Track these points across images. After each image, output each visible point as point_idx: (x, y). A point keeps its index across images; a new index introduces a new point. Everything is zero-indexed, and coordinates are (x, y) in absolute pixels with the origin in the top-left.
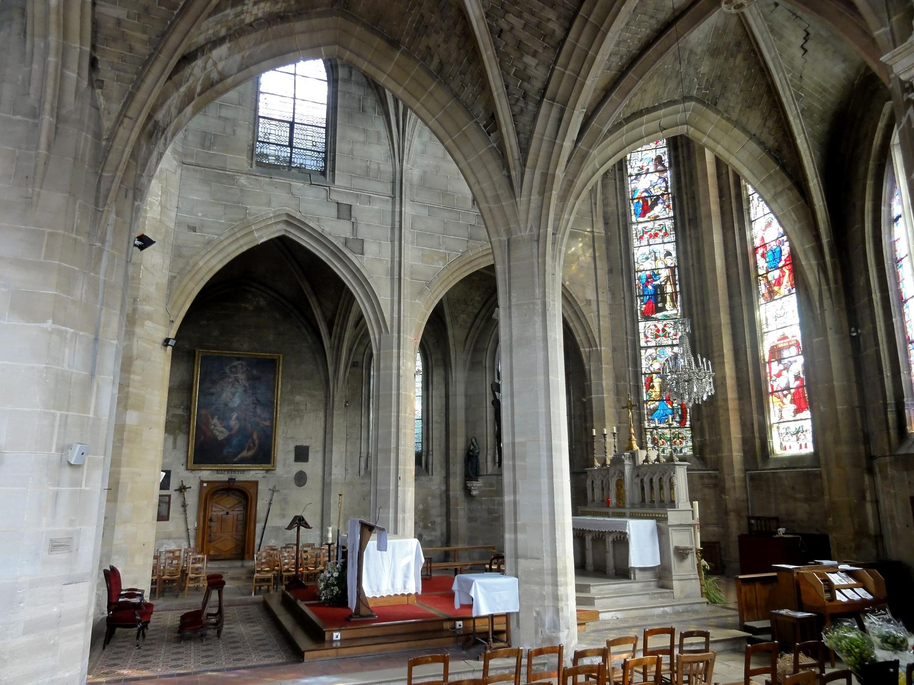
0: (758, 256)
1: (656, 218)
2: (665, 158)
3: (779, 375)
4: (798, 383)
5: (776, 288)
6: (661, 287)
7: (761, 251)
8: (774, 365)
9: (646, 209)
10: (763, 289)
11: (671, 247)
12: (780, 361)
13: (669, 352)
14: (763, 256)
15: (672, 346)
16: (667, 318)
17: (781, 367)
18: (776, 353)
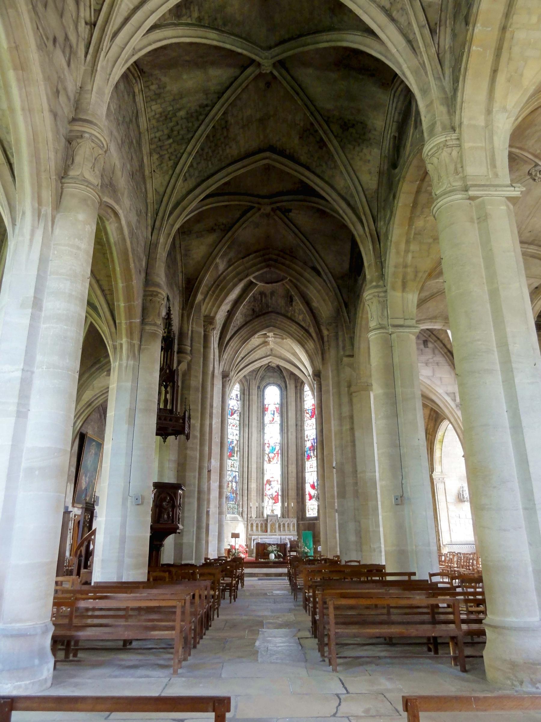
0: (266, 446)
1: (234, 419)
2: (239, 396)
3: (269, 490)
4: (276, 494)
5: (272, 460)
6: (233, 447)
7: (267, 445)
8: (268, 485)
9: (232, 414)
10: (266, 458)
11: (238, 432)
12: (270, 485)
13: (234, 474)
14: (268, 447)
15: (235, 472)
16: (234, 460)
17: (270, 487)
18: (269, 482)
